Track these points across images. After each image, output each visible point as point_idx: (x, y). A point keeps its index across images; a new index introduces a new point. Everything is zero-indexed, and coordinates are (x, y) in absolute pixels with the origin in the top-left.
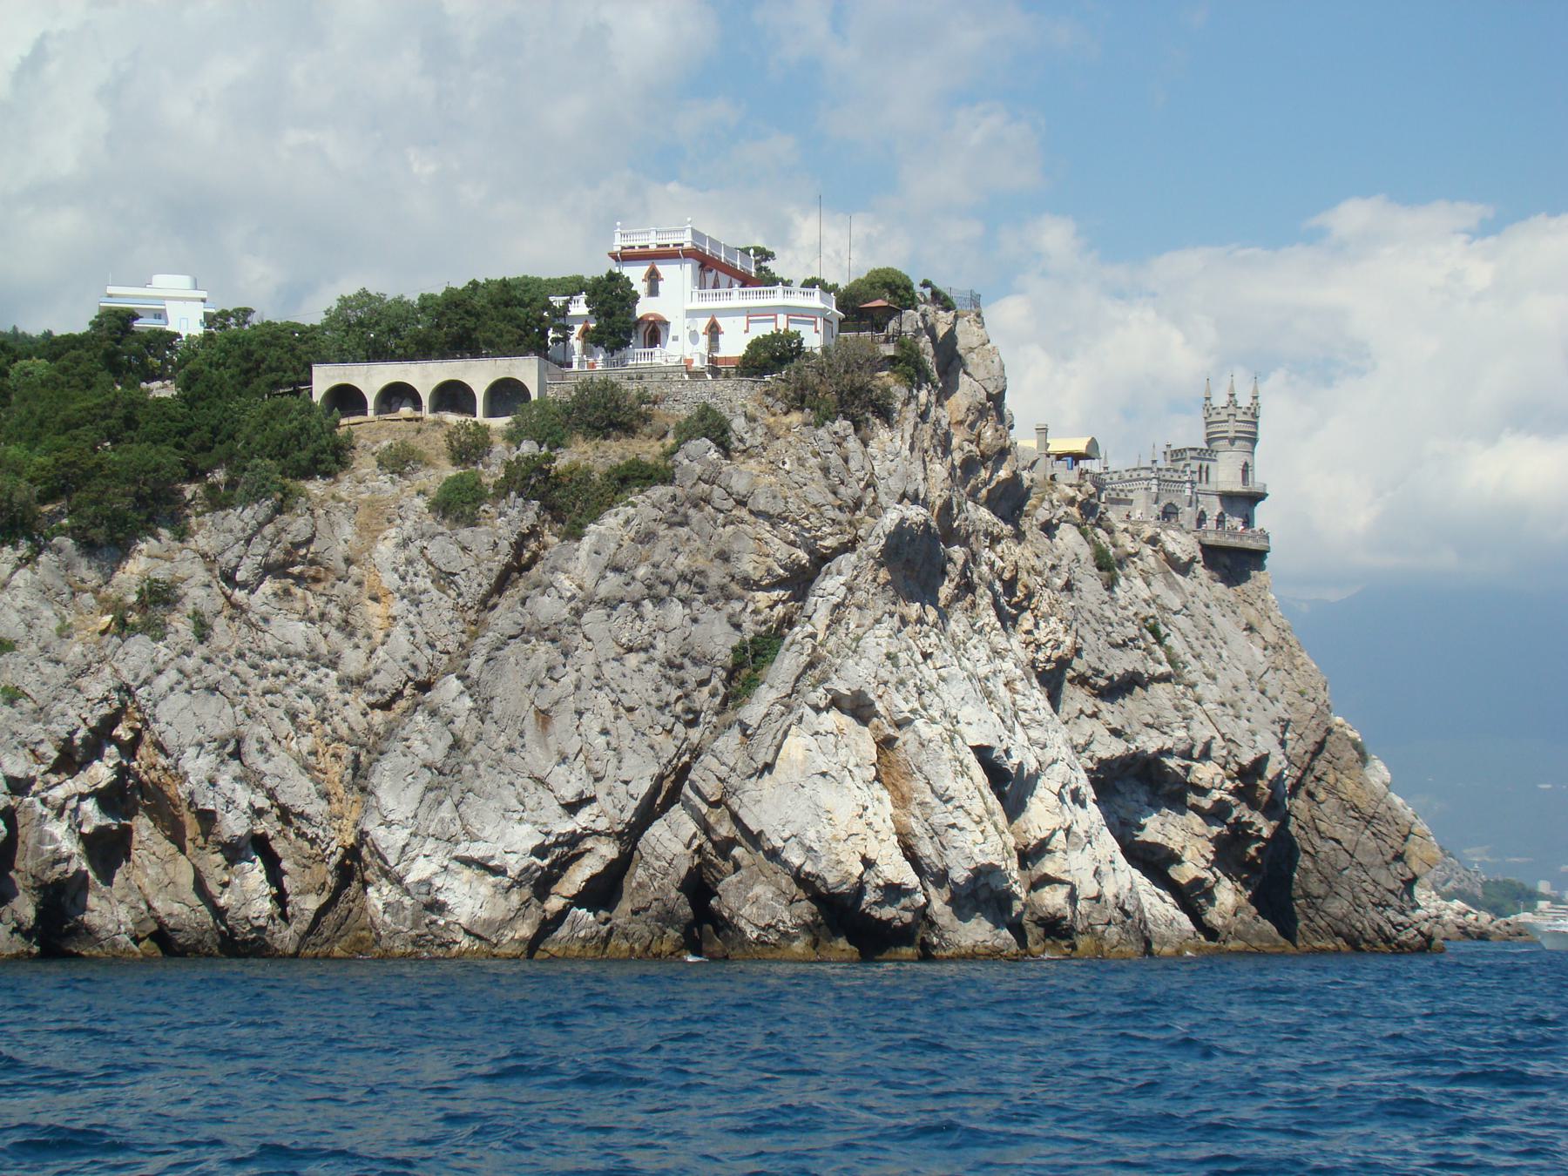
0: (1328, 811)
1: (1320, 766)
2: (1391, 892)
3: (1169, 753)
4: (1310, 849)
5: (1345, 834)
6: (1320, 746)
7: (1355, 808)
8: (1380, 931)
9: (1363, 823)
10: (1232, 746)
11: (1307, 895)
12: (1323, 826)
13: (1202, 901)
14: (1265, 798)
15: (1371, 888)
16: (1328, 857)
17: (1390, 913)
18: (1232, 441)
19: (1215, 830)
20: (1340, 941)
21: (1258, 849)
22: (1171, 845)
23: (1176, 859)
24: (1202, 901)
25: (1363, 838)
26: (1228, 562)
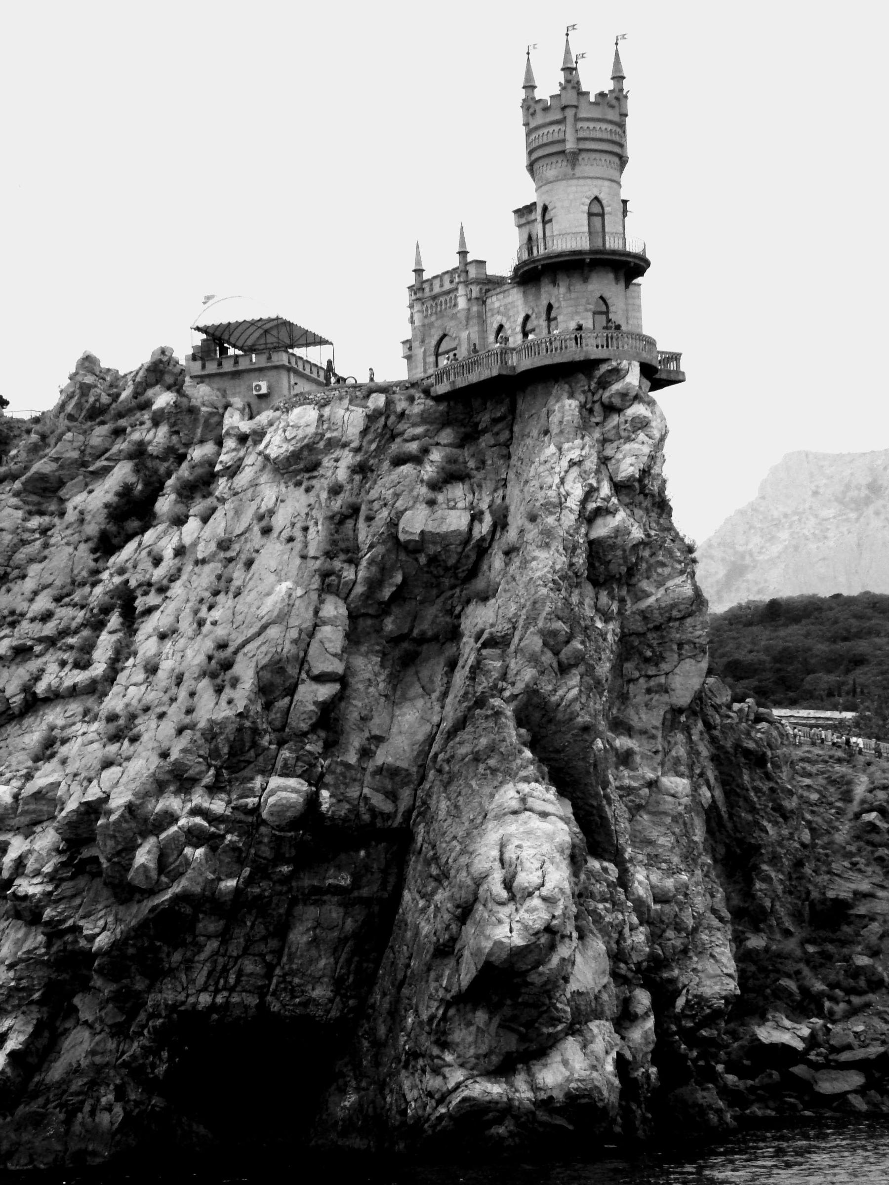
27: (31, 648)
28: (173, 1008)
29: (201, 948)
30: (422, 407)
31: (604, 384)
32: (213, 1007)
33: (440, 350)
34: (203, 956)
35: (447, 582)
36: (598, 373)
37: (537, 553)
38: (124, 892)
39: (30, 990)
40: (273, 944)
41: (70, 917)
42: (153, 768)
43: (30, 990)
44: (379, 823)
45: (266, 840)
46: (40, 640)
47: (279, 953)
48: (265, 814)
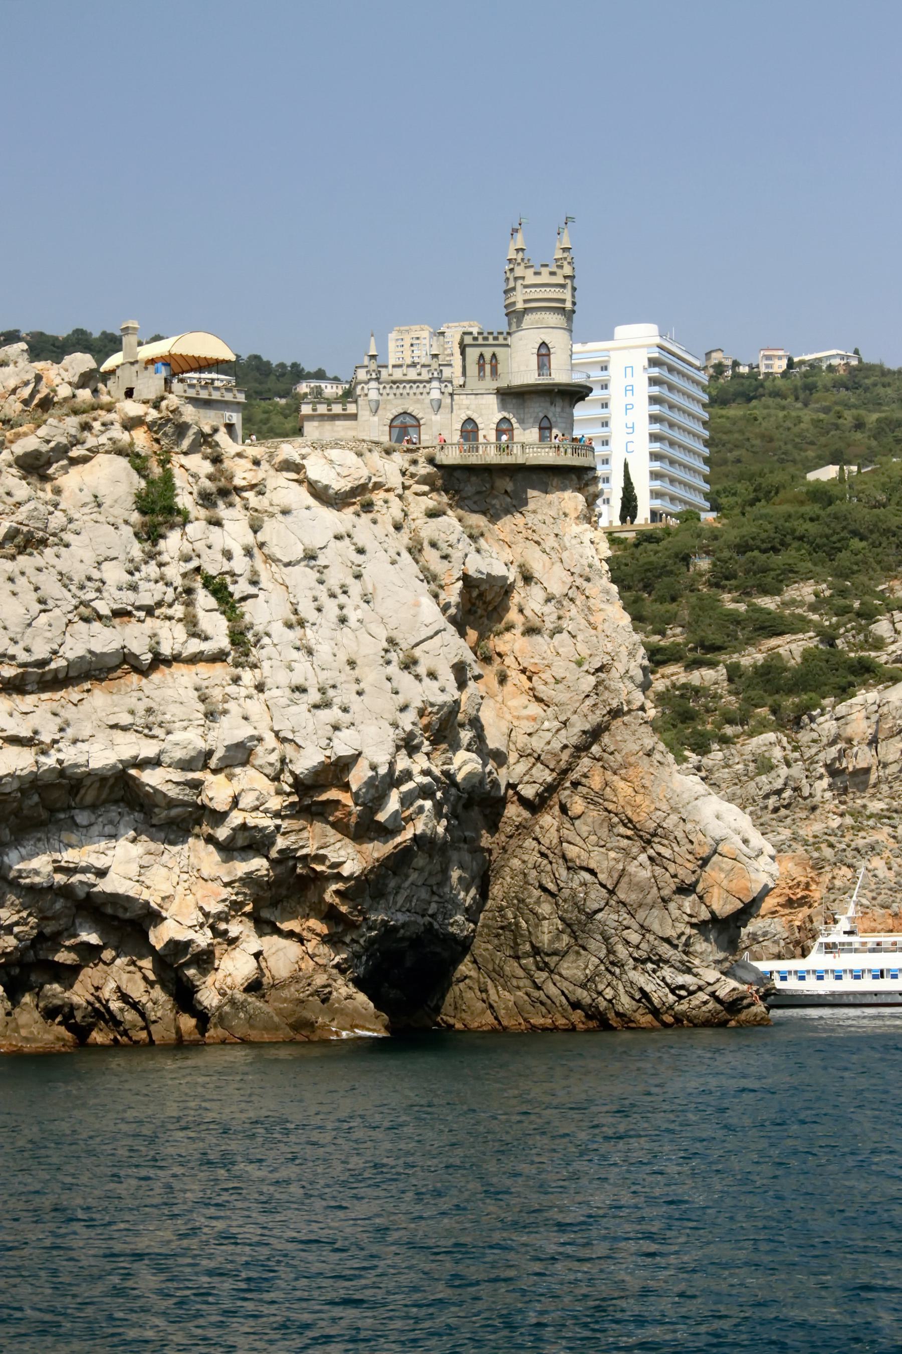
0: (584, 830)
1: (585, 762)
2: (667, 940)
3: (155, 762)
4: (551, 886)
5: (604, 861)
6: (595, 734)
7: (628, 822)
9: (640, 843)
10: (289, 749)
12: (572, 851)
13: (191, 972)
14: (353, 820)
15: (634, 937)
16: (574, 896)
17: (666, 971)
20: (577, 1016)
21: (337, 892)
22: (145, 896)
23: (154, 917)
24: (191, 972)
25: (632, 868)
26: (510, 487)
27: (129, 614)
28: (384, 923)
29: (407, 876)
31: (587, 485)
32: (404, 925)
33: (395, 424)
34: (407, 884)
35: (480, 611)
36: (586, 477)
37: (602, 606)
38: (365, 829)
39: (242, 904)
40: (439, 877)
41: (302, 847)
42: (393, 736)
43: (242, 904)
44: (492, 794)
45: (452, 798)
46: (139, 608)
47: (440, 884)
48: (459, 778)
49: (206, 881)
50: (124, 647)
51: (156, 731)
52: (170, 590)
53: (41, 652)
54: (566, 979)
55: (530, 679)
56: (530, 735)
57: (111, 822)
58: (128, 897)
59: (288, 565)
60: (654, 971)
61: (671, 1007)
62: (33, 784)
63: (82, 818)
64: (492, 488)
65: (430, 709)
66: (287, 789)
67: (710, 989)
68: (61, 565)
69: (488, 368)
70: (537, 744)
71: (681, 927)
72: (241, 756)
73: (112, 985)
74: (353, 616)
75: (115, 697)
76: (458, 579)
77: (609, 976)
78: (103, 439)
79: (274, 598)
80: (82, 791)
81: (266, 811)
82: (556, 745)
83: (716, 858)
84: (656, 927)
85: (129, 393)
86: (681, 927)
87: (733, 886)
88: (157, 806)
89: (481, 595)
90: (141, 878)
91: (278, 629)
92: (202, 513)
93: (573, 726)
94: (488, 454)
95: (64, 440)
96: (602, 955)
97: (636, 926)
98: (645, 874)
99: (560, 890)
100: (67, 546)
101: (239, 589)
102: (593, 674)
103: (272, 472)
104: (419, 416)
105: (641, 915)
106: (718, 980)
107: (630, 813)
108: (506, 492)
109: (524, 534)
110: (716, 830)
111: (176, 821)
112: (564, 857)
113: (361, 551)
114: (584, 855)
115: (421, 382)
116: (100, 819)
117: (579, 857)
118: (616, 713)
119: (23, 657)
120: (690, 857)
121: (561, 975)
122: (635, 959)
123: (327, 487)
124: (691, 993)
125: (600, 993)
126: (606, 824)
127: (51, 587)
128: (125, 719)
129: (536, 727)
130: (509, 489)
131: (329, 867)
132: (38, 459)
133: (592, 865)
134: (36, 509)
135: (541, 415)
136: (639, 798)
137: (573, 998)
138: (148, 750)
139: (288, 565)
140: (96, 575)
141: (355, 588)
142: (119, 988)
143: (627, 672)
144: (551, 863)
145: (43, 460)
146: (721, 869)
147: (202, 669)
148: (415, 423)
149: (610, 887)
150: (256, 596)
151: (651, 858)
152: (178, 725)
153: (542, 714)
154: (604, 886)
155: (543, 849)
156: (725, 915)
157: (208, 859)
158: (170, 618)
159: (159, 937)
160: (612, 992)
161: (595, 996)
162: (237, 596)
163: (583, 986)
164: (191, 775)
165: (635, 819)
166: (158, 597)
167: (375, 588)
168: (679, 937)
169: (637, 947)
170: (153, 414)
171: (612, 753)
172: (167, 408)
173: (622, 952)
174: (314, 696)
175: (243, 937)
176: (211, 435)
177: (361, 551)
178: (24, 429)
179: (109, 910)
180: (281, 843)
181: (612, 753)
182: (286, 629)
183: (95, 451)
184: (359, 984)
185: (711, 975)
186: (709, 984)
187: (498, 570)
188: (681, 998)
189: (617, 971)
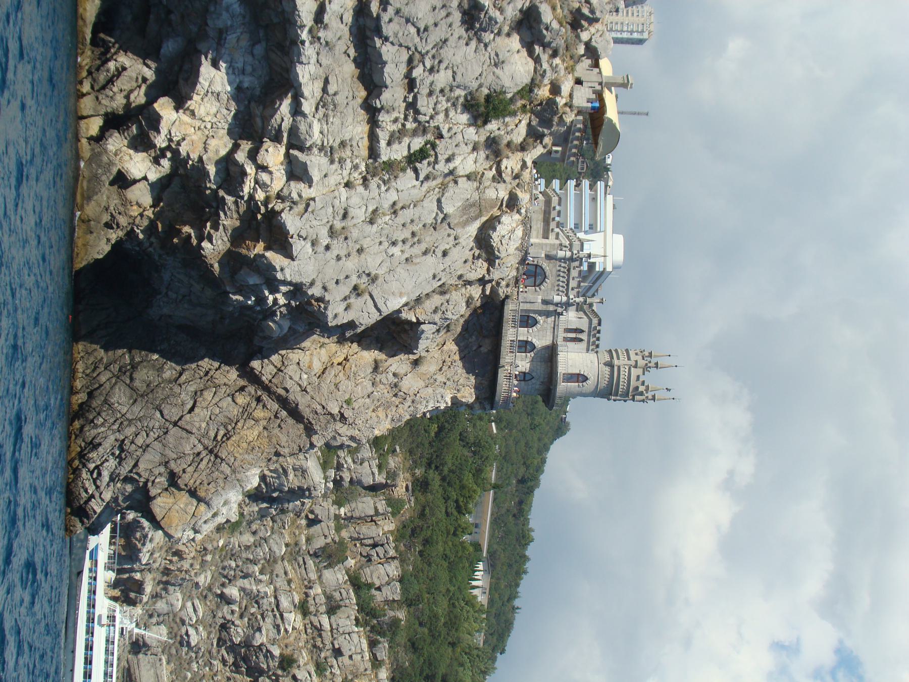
2: (136, 465)
3: (296, 111)
4: (183, 378)
5: (199, 420)
6: (295, 413)
7: (227, 436)
8: (94, 445)
10: (301, 207)
11: (134, 367)
12: (208, 395)
13: (134, 129)
14: (244, 251)
15: (140, 441)
17: (112, 463)
18: (610, 365)
19: (212, 169)
20: (82, 397)
21: (189, 236)
23: (180, 103)
24: (134, 129)
25: (193, 440)
26: (484, 350)
30: (501, 294)
31: (480, 403)
37: (390, 416)
41: (225, 214)
46: (415, 98)
49: (205, 143)
50: (386, 87)
51: (322, 111)
52: (428, 118)
53: (388, 30)
54: (112, 388)
55: (339, 364)
56: (298, 363)
57: (254, 70)
58: (196, 84)
59: (439, 201)
60: (113, 454)
61: (84, 466)
62: (286, 21)
63: (259, 50)
64: (484, 337)
65: (322, 306)
66: (270, 206)
67: (97, 495)
68: (452, 42)
69: (573, 335)
70: (291, 370)
71: (145, 475)
72: (298, 171)
73: (127, 63)
74: (396, 250)
75: (349, 79)
76: (417, 319)
77: (112, 420)
78: (545, 66)
79: (416, 191)
80: (279, 53)
81: (255, 189)
82: (289, 384)
83: (195, 502)
84: (148, 456)
85: (579, 82)
86: (145, 475)
87: (174, 513)
88: (264, 108)
89: (406, 331)
90: (210, 94)
91: (392, 196)
92: (483, 139)
93: (303, 396)
94: (511, 334)
95: (547, 39)
96: (129, 416)
97: (148, 442)
98: (188, 449)
99: (180, 385)
100: (467, 44)
101: (424, 168)
102: (339, 412)
103: (509, 186)
104: (542, 287)
105: (157, 445)
106: (103, 500)
107: (233, 439)
108: (480, 346)
109: (447, 359)
110: (217, 502)
111: (250, 125)
112: (206, 388)
113: (445, 254)
114: (204, 404)
115: (567, 290)
116: (257, 62)
117: (204, 400)
118: (310, 430)
119: (385, 17)
120: (198, 483)
121: (116, 383)
122: (123, 440)
123: (494, 229)
124: (95, 481)
125: (99, 414)
126: (227, 421)
127: (435, 36)
128: (332, 89)
129: (304, 369)
130: (482, 349)
131: (209, 232)
132: (535, 20)
133: (196, 410)
134: (496, 23)
135: (534, 374)
136: (245, 445)
137: (96, 393)
138: (307, 107)
139: (439, 201)
140: (443, 66)
141: (418, 250)
142: (124, 69)
143: (339, 435)
144: (201, 378)
145: (534, 25)
146: (187, 505)
147: (365, 142)
148: (537, 283)
149: (179, 424)
150: (417, 179)
151: (199, 454)
152: (325, 127)
153: (313, 373)
154: (180, 419)
155: (211, 373)
156: (152, 507)
157: (221, 145)
158: (406, 119)
159: (164, 107)
160: (99, 423)
161: (97, 410)
162: (418, 165)
163: (106, 401)
164: (285, 135)
165: (229, 442)
166: (422, 110)
167: (416, 264)
168: (137, 474)
169: (132, 442)
170: (561, 101)
171: (279, 426)
172: (564, 113)
173: (130, 431)
174: (338, 225)
175: (160, 168)
176: (541, 143)
177: (445, 254)
178: (559, 10)
179: (186, 67)
180: (230, 199)
181: (279, 426)
182: (391, 202)
183: (537, 60)
184: (118, 247)
185: (108, 496)
186: (101, 494)
187: (423, 344)
188: (92, 473)
189: (116, 427)
